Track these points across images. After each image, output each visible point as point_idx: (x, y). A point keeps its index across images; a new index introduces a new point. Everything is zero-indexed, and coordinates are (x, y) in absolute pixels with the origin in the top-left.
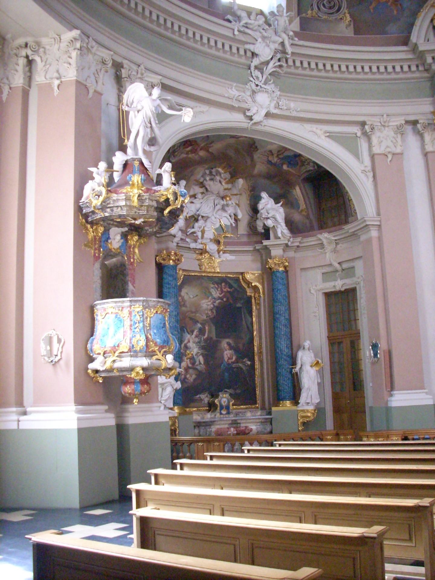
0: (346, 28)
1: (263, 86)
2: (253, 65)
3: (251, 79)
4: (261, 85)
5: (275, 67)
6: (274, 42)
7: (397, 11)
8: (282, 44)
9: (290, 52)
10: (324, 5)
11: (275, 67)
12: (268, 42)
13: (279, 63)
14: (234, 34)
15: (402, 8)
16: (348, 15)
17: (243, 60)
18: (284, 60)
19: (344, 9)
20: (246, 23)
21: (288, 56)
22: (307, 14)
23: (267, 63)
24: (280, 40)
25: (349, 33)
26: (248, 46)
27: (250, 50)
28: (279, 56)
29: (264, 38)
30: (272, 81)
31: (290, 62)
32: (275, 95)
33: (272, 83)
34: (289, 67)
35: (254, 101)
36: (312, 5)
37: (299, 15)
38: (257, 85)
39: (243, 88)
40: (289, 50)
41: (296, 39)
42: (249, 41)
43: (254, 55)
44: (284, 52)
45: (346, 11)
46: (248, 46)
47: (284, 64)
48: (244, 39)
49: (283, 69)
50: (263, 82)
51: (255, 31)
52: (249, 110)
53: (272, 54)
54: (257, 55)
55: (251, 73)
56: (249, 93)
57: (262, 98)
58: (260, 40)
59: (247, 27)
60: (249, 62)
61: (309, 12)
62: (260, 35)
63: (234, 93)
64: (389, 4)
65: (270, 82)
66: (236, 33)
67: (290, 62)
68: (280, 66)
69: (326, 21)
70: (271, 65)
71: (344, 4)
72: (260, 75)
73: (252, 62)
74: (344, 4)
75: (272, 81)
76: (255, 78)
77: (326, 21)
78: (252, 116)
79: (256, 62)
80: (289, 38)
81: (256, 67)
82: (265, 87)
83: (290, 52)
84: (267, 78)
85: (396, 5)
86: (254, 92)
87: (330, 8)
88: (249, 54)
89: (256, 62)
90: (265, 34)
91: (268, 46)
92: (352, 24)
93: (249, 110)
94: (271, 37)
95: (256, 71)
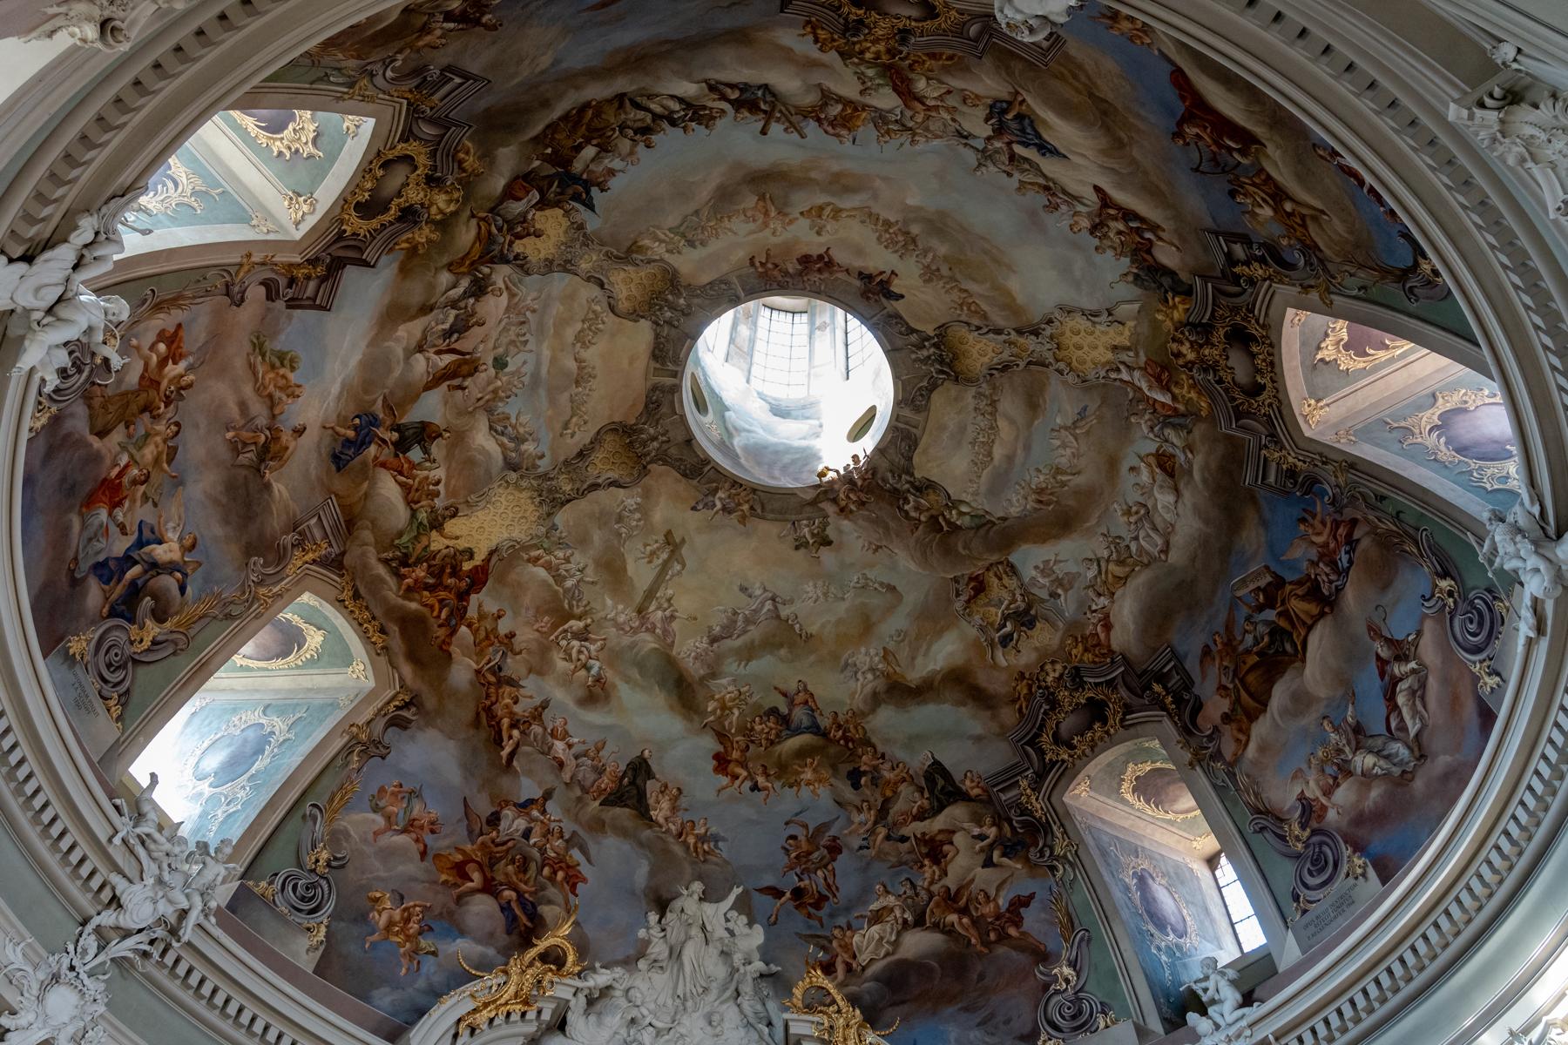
0: (308, 950)
1: (83, 976)
2: (96, 921)
3: (71, 948)
4: (81, 971)
5: (135, 951)
6: (170, 902)
7: (408, 969)
8: (183, 914)
9: (185, 939)
10: (295, 888)
11: (135, 951)
12: (160, 894)
13: (147, 948)
14: (110, 840)
15: (418, 969)
16: (323, 930)
17: (85, 901)
18: (162, 946)
19: (323, 916)
20: (148, 835)
21: (175, 944)
22: (258, 886)
23: (126, 934)
24: (185, 905)
25: (307, 963)
26: (115, 879)
27: (113, 889)
28: (160, 932)
29: (160, 881)
30: (106, 977)
31: (169, 959)
32: (95, 1007)
33: (104, 981)
34: (161, 965)
35: (40, 999)
36: (276, 874)
37: (243, 877)
38: (72, 968)
39: (40, 957)
40: (188, 933)
41: (213, 920)
42: (127, 871)
43: (115, 902)
44: (174, 932)
45: (325, 921)
46: (115, 879)
47: (156, 956)
48: (120, 861)
49: (146, 963)
50: (87, 967)
51: (154, 859)
52: (13, 1013)
53: (150, 921)
54: (120, 906)
55: (80, 935)
56: (41, 975)
57: (62, 1001)
58: (150, 881)
59: (143, 843)
60: (92, 912)
61: (263, 884)
62: (157, 872)
63: (12, 958)
64: (402, 950)
65: (101, 977)
66: (117, 840)
67: (169, 959)
68: (145, 955)
69: (280, 917)
70: (130, 942)
71: (329, 907)
72: (93, 951)
73: (99, 914)
74: (329, 907)
75: (106, 977)
76: (79, 950)
77: (280, 917)
78: (8, 1030)
79: (108, 918)
80: (203, 911)
81: (98, 930)
82: (87, 981)
83: (185, 939)
84: (104, 963)
85: (411, 959)
86: (56, 978)
87: (303, 899)
88: (106, 895)
89: (108, 918)
90: (166, 877)
91: (155, 903)
92: (322, 948)
93: (13, 1013)
94: (172, 888)
95: (93, 937)
